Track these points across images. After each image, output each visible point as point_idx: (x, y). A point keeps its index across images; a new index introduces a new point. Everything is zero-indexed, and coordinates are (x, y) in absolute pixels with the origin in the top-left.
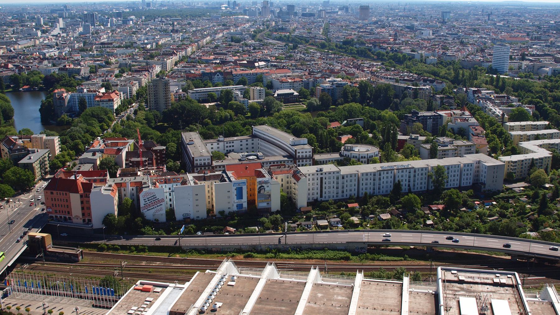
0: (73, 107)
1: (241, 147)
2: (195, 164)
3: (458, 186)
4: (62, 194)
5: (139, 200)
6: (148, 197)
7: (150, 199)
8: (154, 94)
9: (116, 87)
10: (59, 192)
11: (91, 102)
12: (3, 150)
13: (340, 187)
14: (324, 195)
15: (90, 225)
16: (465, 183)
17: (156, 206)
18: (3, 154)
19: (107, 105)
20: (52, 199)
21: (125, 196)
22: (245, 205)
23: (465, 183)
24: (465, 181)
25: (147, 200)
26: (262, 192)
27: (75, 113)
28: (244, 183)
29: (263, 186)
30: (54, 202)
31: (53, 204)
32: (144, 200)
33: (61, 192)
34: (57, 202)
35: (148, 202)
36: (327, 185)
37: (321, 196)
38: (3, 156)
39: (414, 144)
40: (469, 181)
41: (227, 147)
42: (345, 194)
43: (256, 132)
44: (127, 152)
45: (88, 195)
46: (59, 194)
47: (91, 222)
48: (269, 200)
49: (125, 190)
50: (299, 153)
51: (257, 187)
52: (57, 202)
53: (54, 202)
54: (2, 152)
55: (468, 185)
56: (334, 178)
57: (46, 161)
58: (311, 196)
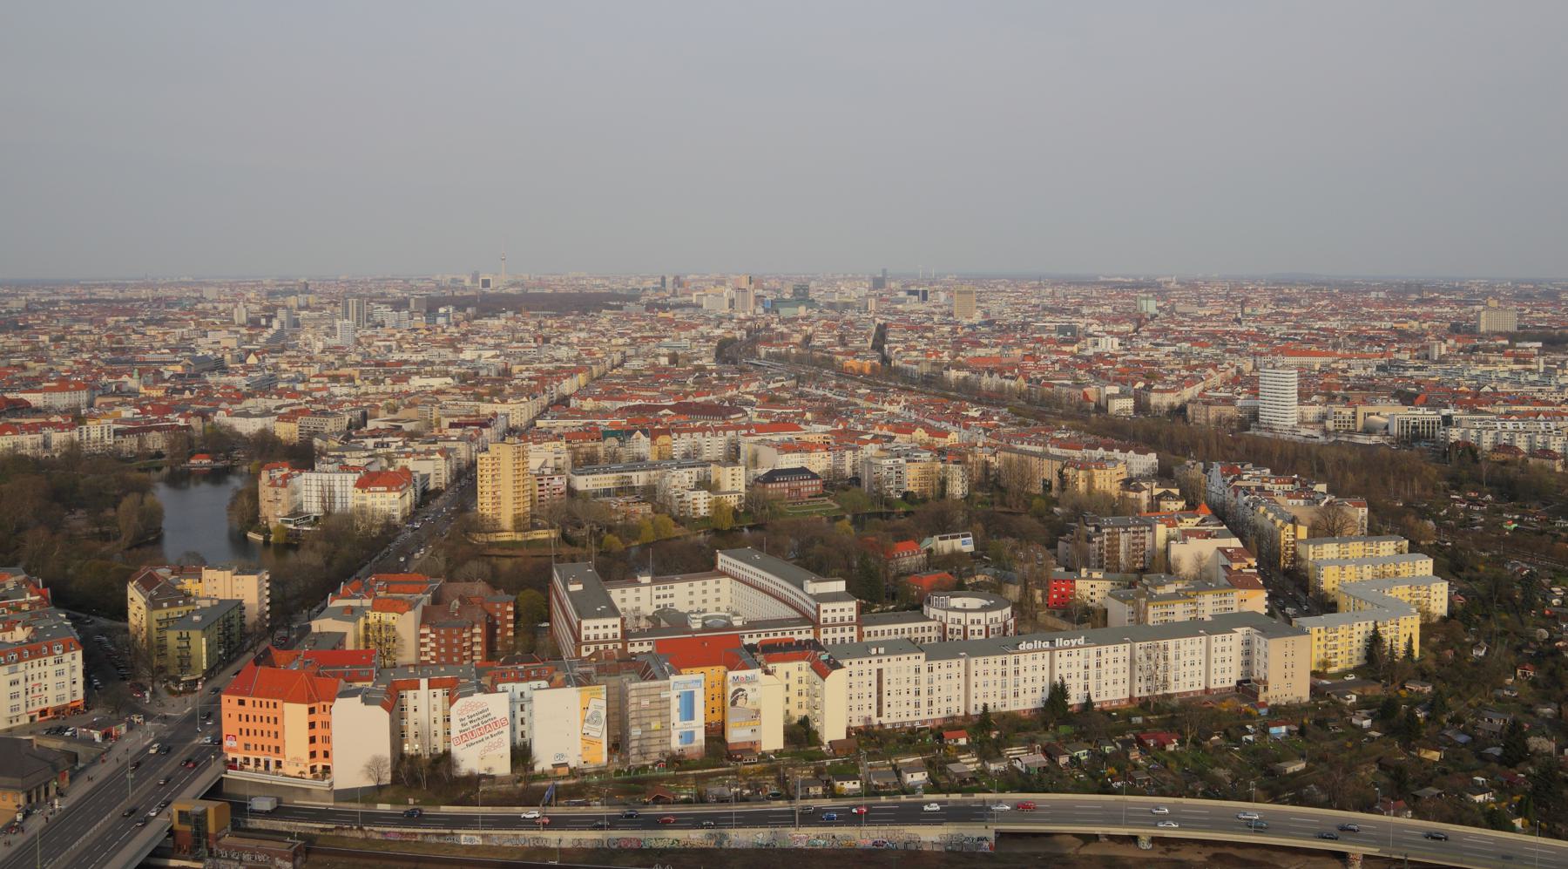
0: (304, 504)
1: (691, 598)
2: (583, 638)
3: (1203, 687)
4: (264, 705)
5: (449, 720)
6: (471, 714)
7: (474, 718)
8: (493, 476)
9: (406, 460)
10: (258, 700)
11: (346, 492)
12: (132, 599)
13: (924, 692)
14: (885, 710)
15: (327, 781)
16: (1218, 681)
17: (488, 735)
18: (132, 609)
19: (383, 499)
20: (240, 716)
21: (415, 710)
22: (700, 736)
23: (1218, 681)
24: (1219, 677)
25: (467, 721)
26: (740, 702)
27: (308, 518)
28: (697, 681)
29: (743, 690)
30: (244, 725)
31: (241, 730)
32: (461, 720)
33: (264, 701)
34: (251, 725)
35: (470, 725)
36: (893, 688)
37: (880, 714)
38: (131, 616)
39: (1093, 590)
40: (1227, 676)
41: (658, 597)
42: (935, 708)
43: (724, 565)
44: (424, 607)
45: (327, 708)
46: (258, 704)
47: (329, 773)
48: (757, 723)
49: (415, 697)
50: (825, 611)
51: (731, 689)
52: (251, 725)
53: (244, 725)
54: (129, 606)
55: (1227, 685)
56: (908, 670)
57: (233, 626)
58: (855, 714)
